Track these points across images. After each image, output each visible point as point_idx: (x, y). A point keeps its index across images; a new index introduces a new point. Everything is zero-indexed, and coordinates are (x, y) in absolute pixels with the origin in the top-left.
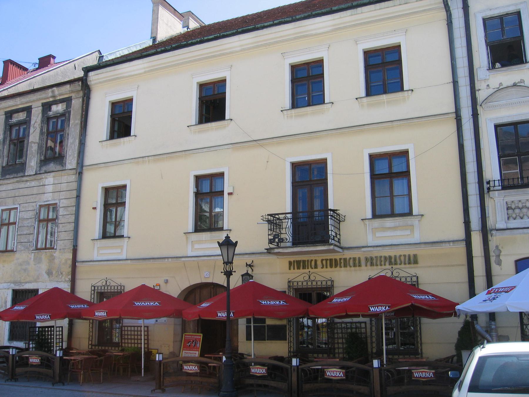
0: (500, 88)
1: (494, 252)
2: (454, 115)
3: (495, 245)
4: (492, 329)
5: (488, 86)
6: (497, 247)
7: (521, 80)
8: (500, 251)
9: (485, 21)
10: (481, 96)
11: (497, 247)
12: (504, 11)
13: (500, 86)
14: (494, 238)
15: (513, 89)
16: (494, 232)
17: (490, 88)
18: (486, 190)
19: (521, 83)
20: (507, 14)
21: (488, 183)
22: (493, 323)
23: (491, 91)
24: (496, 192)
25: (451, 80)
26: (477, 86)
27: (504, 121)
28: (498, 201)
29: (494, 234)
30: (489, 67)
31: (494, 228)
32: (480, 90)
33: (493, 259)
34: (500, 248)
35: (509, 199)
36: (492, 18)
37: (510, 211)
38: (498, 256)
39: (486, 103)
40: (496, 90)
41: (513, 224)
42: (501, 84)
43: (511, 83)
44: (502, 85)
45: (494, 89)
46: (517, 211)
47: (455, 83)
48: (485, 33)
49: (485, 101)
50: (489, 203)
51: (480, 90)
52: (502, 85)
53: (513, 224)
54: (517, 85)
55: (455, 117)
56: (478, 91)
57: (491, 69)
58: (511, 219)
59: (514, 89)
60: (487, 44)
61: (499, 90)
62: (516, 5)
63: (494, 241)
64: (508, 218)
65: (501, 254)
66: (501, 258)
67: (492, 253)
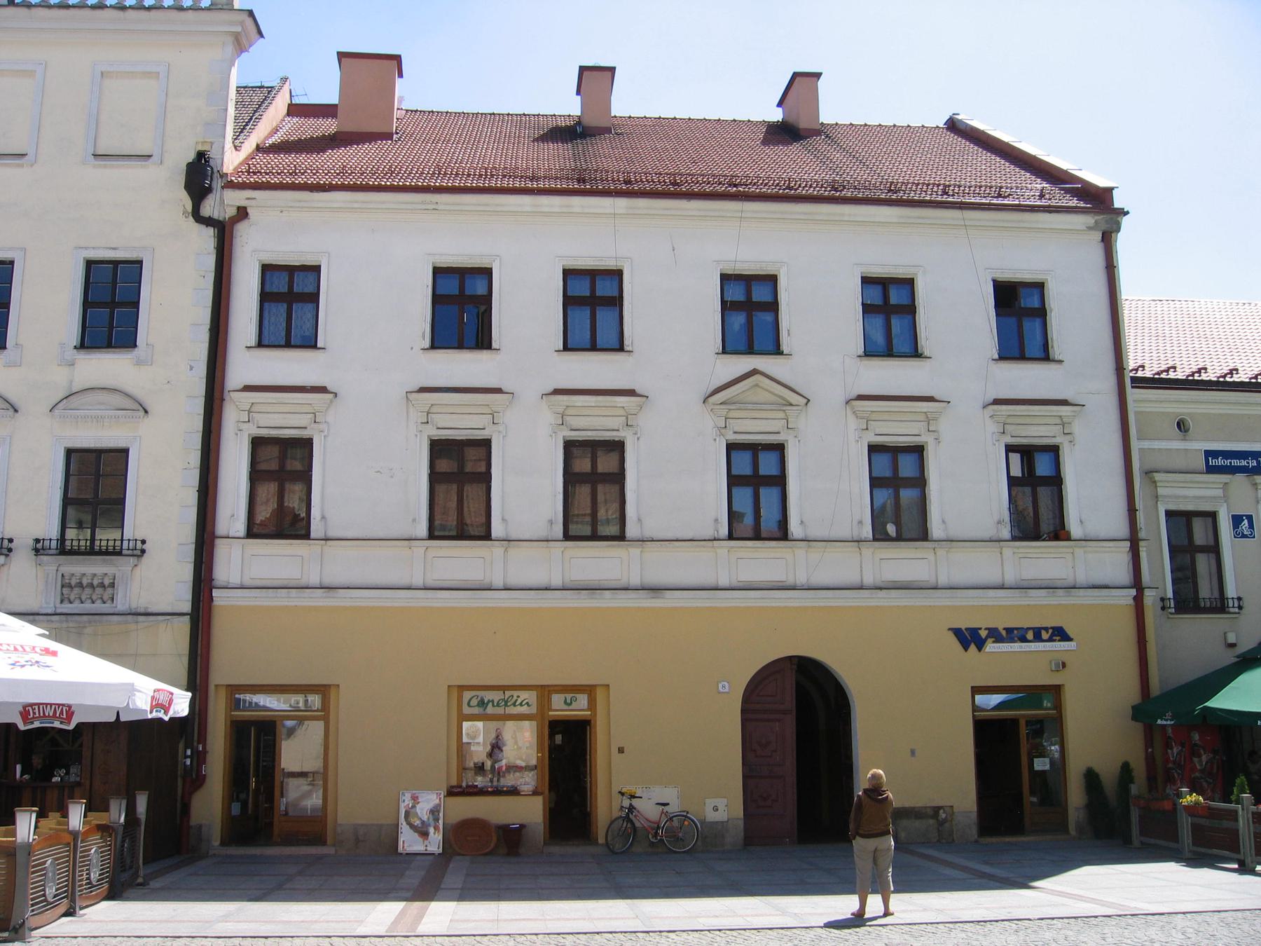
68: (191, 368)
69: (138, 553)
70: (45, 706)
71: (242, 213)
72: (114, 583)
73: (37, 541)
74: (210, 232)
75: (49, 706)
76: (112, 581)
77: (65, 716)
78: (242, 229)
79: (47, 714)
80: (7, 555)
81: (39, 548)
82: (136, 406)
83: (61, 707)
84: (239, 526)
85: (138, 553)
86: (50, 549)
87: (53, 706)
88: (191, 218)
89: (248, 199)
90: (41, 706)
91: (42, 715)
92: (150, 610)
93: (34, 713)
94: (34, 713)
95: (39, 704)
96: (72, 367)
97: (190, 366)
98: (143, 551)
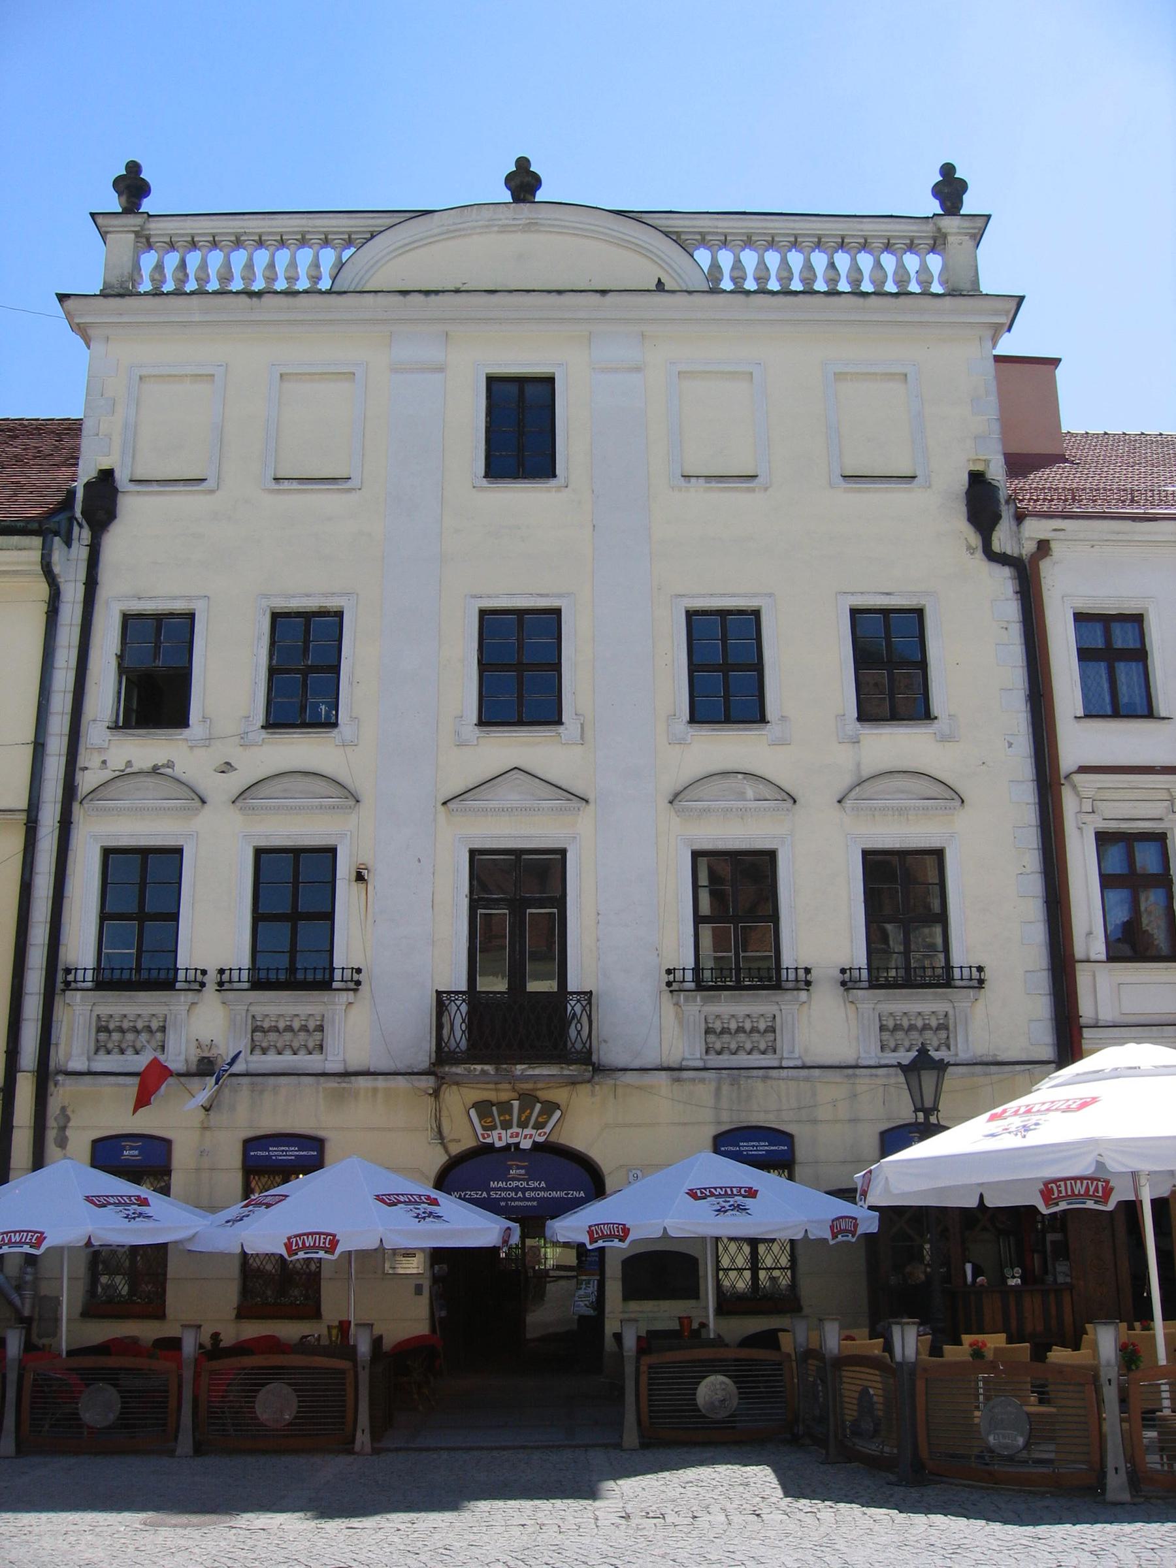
0: (129, 770)
1: (56, 1119)
2: (23, 817)
3: (61, 1105)
4: (26, 1283)
5: (104, 762)
6: (63, 1109)
7: (169, 761)
8: (68, 1119)
9: (128, 620)
10: (87, 781)
11: (63, 1109)
12: (165, 608)
13: (126, 767)
14: (61, 1090)
15: (149, 779)
16: (60, 1078)
17: (106, 768)
18: (60, 986)
19: (168, 767)
20: (172, 615)
21: (68, 971)
22: (29, 1270)
23: (107, 775)
24: (79, 994)
25: (30, 737)
26: (82, 761)
27: (120, 844)
28: (81, 1012)
29: (61, 1082)
30: (117, 721)
31: (63, 1068)
32: (86, 768)
33: (51, 1135)
34: (69, 1113)
35: (104, 1010)
36: (140, 616)
37: (103, 1036)
38: (63, 1128)
39: (90, 801)
40: (117, 773)
41: (103, 1063)
42: (129, 764)
43: (147, 765)
44: (131, 767)
45: (114, 771)
46: (116, 1036)
47: (39, 747)
48: (122, 646)
49: (90, 797)
50: (61, 1013)
51: (86, 768)
52: (131, 767)
53: (103, 1063)
54: (158, 771)
55: (25, 822)
56: (84, 770)
57: (121, 728)
58: (102, 1052)
59: (151, 781)
60: (122, 670)
61: (122, 776)
62: (189, 598)
63: (61, 1094)
64: (97, 1051)
65: (70, 1124)
66: (68, 1133)
67: (51, 1123)
68: (1010, 745)
69: (975, 983)
70: (1073, 1182)
71: (1044, 547)
72: (322, 1026)
73: (843, 971)
74: (1006, 572)
75: (1078, 1182)
76: (161, 1024)
77: (1100, 1194)
78: (1045, 566)
79: (1076, 1193)
80: (355, 990)
81: (847, 982)
82: (786, 797)
83: (1095, 1183)
84: (1098, 948)
85: (975, 983)
86: (860, 981)
87: (1085, 1182)
88: (979, 554)
89: (1055, 530)
90: (1068, 1182)
91: (1069, 1193)
92: (999, 1059)
93: (1060, 1192)
94: (1060, 1192)
95: (1065, 1180)
96: (857, 744)
97: (1008, 742)
98: (981, 982)
